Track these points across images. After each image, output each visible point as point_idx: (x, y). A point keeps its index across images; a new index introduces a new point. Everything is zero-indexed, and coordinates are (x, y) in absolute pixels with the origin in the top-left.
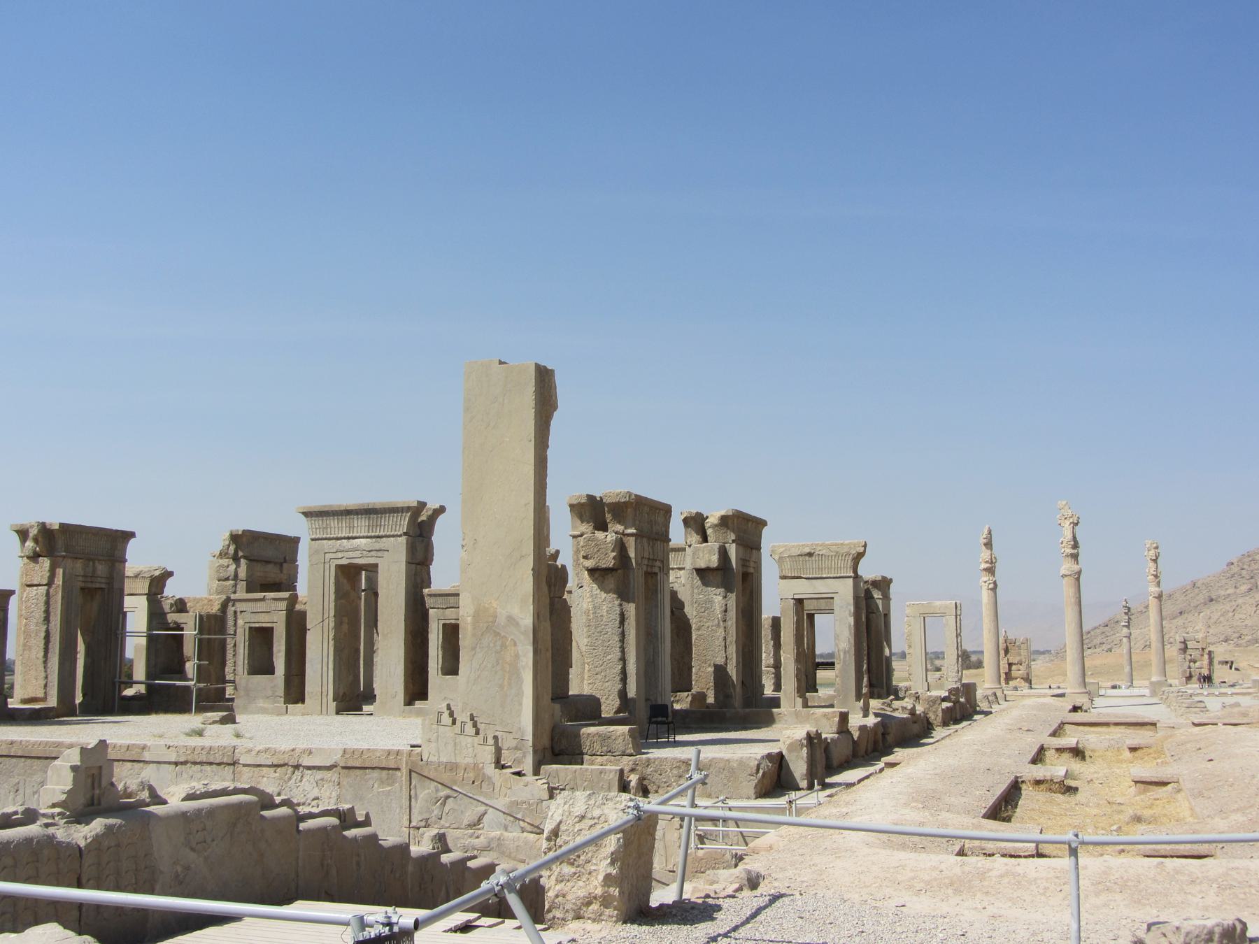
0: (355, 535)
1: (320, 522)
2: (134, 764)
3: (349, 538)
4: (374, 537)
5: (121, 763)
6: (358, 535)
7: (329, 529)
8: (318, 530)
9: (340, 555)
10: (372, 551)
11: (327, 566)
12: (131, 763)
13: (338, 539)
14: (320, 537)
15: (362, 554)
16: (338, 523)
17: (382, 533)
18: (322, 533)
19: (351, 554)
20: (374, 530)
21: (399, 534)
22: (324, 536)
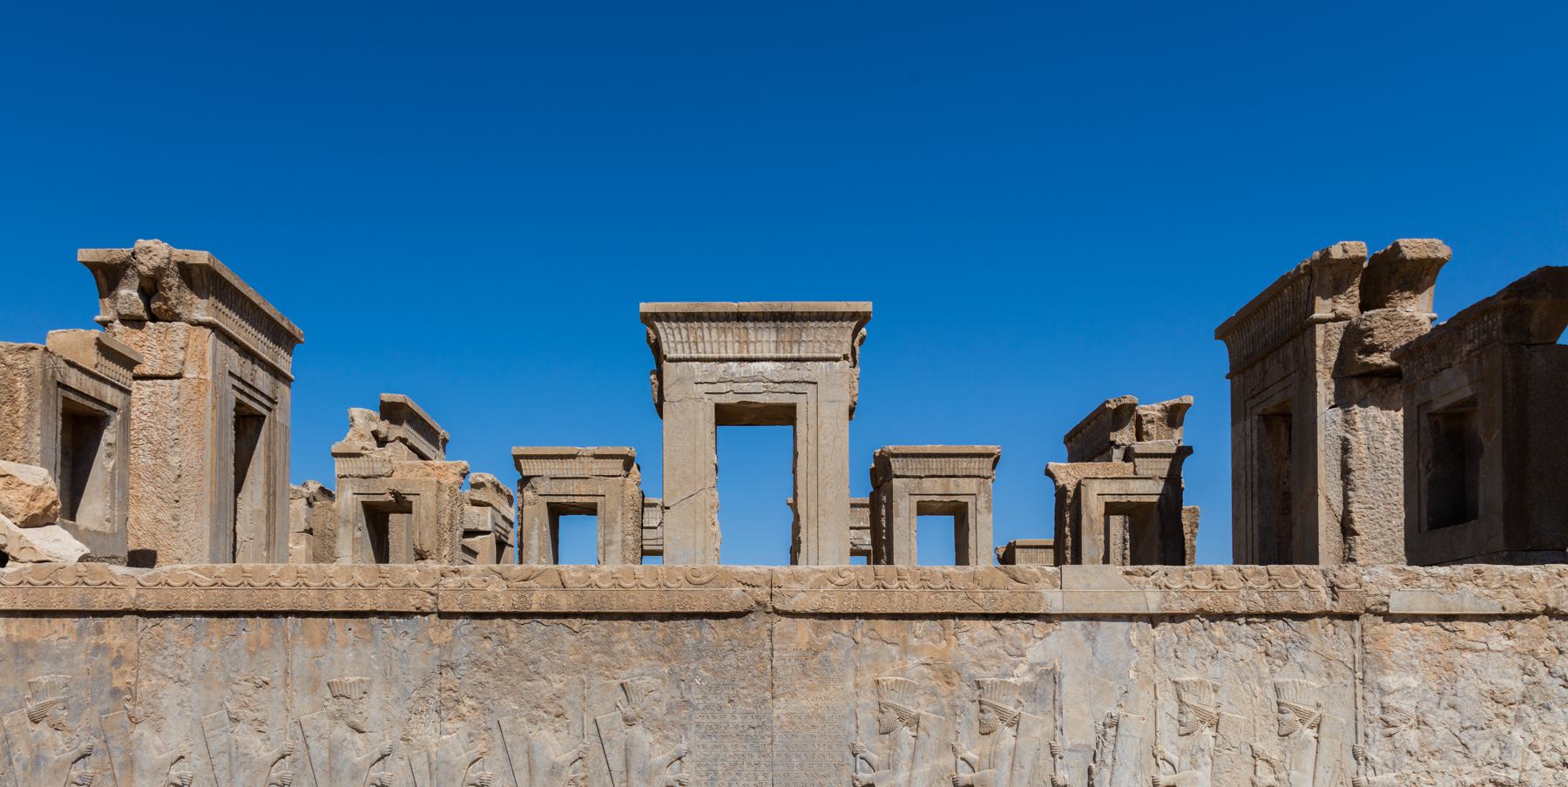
0: (753, 355)
1: (684, 332)
2: (1002, 624)
3: (742, 360)
6: (759, 355)
7: (701, 345)
8: (679, 346)
9: (724, 387)
10: (784, 382)
12: (989, 624)
14: (687, 355)
15: (764, 386)
16: (719, 336)
17: (803, 355)
18: (687, 350)
20: (788, 348)
21: (837, 355)
22: (695, 355)
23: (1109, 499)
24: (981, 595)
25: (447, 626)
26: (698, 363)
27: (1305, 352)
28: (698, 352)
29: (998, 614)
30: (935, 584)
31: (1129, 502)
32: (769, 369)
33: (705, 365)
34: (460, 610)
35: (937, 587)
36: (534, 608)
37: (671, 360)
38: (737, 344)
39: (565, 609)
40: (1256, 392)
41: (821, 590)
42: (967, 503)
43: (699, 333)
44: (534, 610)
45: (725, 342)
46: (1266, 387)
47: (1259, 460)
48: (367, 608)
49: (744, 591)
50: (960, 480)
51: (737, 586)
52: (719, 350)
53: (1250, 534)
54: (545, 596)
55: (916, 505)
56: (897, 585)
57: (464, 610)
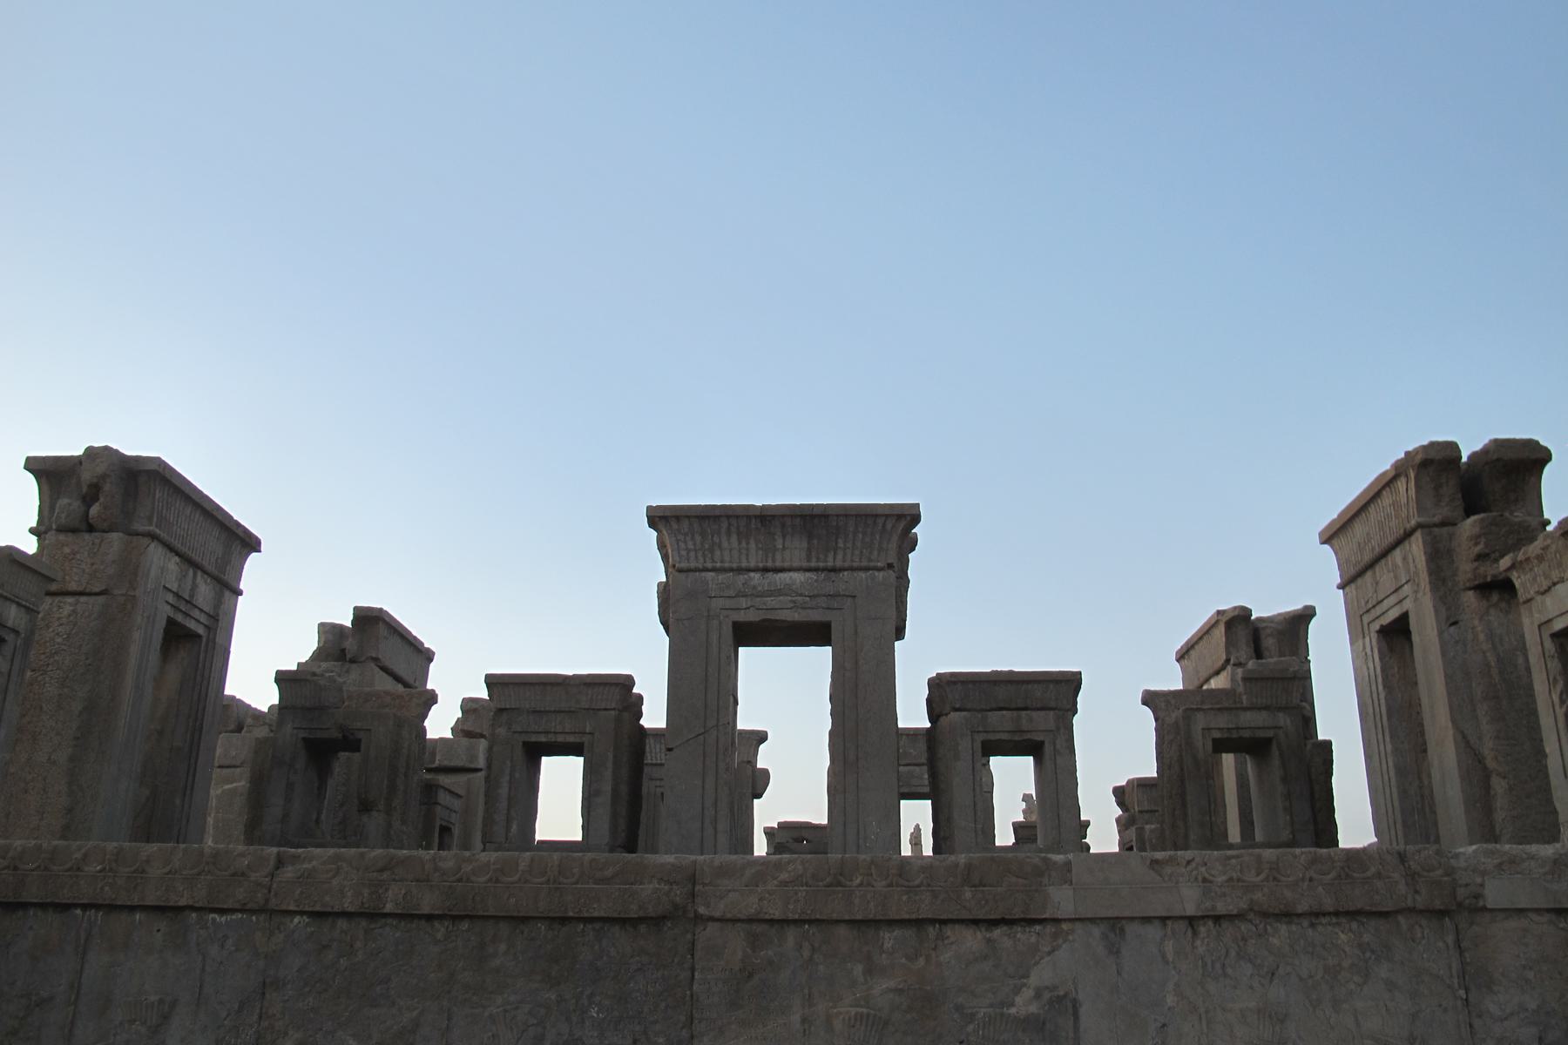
0: (778, 564)
1: (698, 538)
2: (997, 932)
4: (824, 570)
5: (932, 931)
6: (786, 565)
7: (718, 553)
8: (692, 554)
9: (743, 602)
11: (715, 622)
13: (740, 570)
16: (740, 543)
17: (839, 564)
18: (701, 560)
19: (771, 602)
20: (822, 556)
22: (709, 565)
23: (1217, 735)
24: (968, 895)
25: (279, 928)
26: (712, 574)
27: (1414, 561)
28: (713, 561)
29: (991, 920)
30: (908, 881)
31: (1241, 738)
32: (798, 581)
33: (721, 577)
34: (296, 909)
35: (911, 884)
36: (389, 908)
37: (680, 571)
38: (761, 552)
39: (426, 910)
40: (1371, 606)
41: (759, 889)
42: (1042, 743)
43: (716, 539)
44: (388, 911)
45: (747, 549)
46: (1380, 599)
47: (1384, 687)
48: (182, 902)
49: (657, 889)
50: (1034, 714)
51: (650, 883)
52: (740, 559)
53: (1386, 777)
54: (403, 892)
55: (980, 745)
56: (858, 881)
57: (301, 908)
